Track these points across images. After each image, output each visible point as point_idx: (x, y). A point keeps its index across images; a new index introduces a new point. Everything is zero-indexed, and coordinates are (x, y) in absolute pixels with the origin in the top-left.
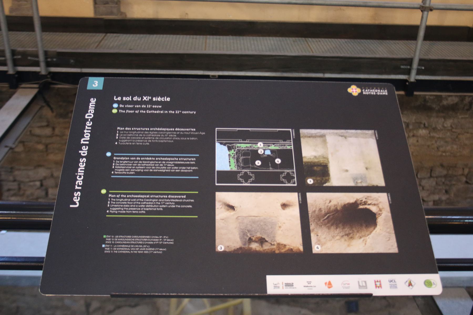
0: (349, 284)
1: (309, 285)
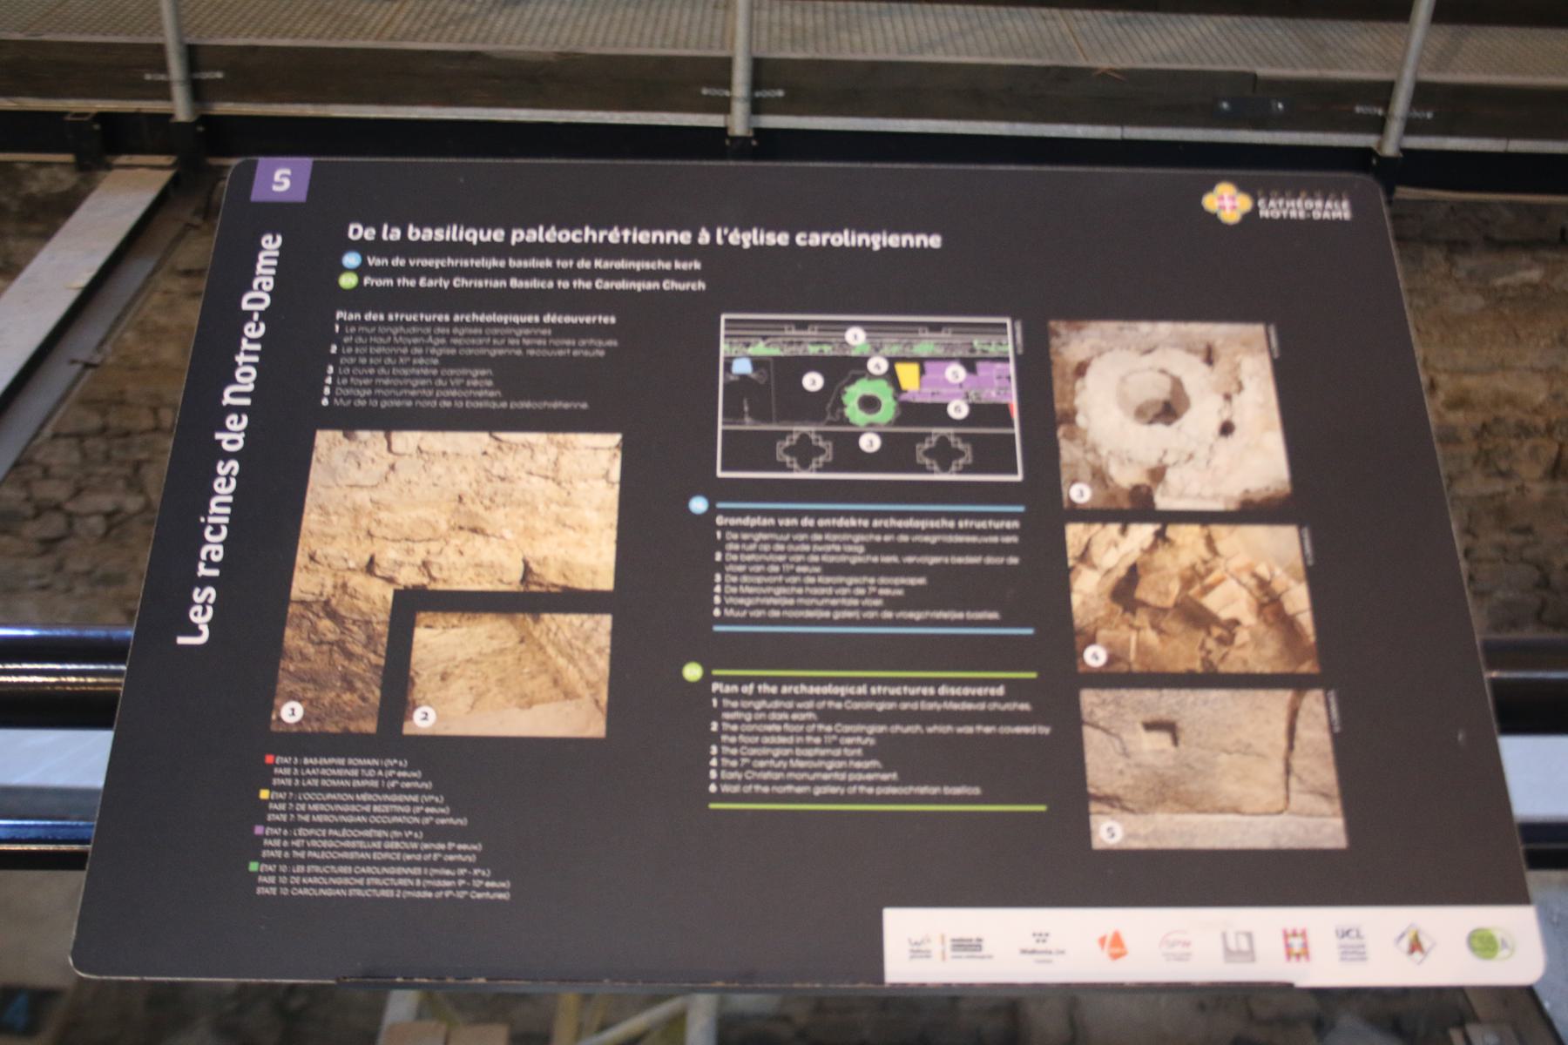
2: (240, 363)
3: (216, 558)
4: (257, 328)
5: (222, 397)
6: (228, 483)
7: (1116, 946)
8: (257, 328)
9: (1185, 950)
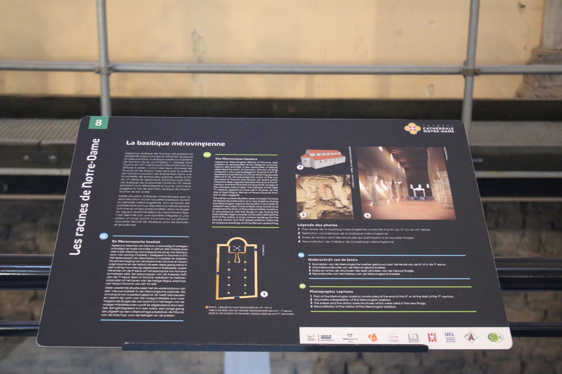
1: (350, 338)
2: (87, 176)
3: (81, 231)
4: (93, 166)
5: (82, 186)
6: (85, 210)
7: (374, 337)
8: (93, 166)
9: (396, 339)
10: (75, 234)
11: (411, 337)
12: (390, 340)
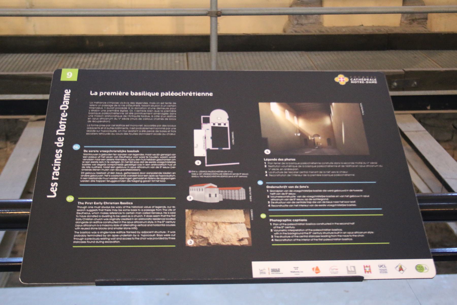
0: (337, 269)
1: (296, 271)
3: (57, 175)
7: (317, 270)
9: (337, 271)
10: (52, 178)
11: (350, 270)
12: (331, 272)
